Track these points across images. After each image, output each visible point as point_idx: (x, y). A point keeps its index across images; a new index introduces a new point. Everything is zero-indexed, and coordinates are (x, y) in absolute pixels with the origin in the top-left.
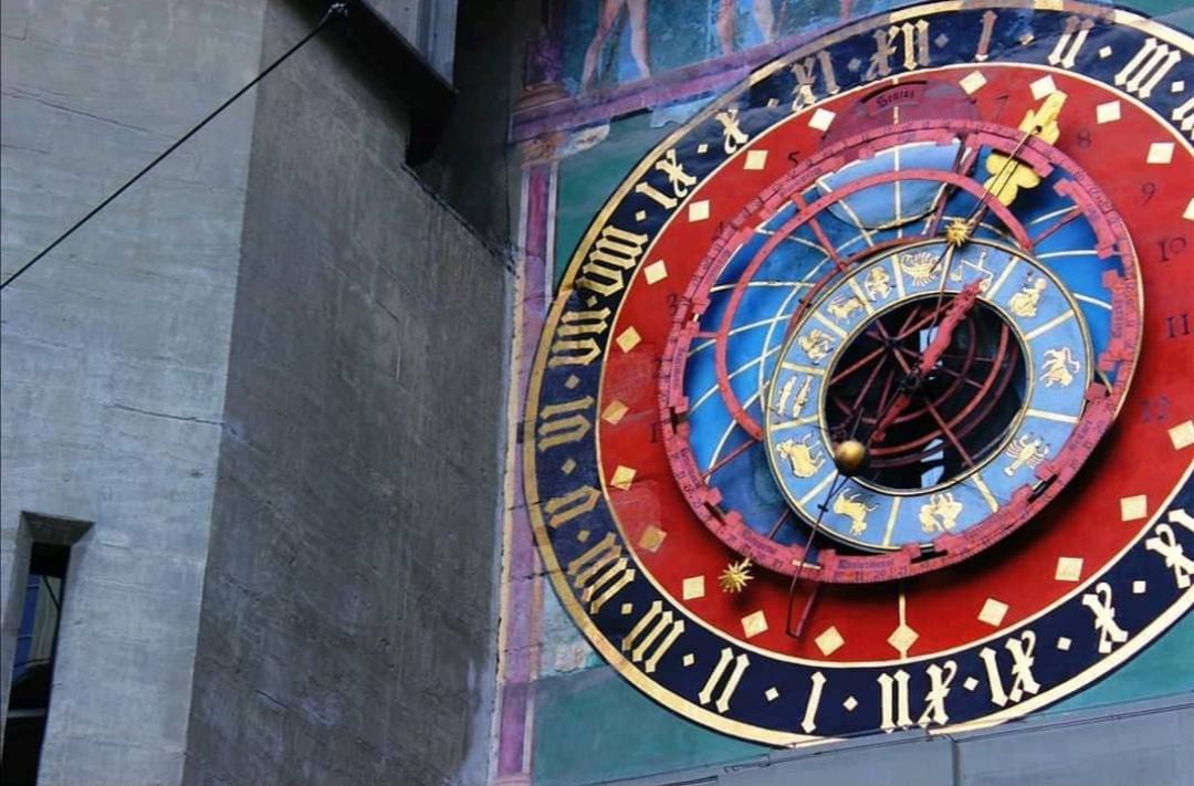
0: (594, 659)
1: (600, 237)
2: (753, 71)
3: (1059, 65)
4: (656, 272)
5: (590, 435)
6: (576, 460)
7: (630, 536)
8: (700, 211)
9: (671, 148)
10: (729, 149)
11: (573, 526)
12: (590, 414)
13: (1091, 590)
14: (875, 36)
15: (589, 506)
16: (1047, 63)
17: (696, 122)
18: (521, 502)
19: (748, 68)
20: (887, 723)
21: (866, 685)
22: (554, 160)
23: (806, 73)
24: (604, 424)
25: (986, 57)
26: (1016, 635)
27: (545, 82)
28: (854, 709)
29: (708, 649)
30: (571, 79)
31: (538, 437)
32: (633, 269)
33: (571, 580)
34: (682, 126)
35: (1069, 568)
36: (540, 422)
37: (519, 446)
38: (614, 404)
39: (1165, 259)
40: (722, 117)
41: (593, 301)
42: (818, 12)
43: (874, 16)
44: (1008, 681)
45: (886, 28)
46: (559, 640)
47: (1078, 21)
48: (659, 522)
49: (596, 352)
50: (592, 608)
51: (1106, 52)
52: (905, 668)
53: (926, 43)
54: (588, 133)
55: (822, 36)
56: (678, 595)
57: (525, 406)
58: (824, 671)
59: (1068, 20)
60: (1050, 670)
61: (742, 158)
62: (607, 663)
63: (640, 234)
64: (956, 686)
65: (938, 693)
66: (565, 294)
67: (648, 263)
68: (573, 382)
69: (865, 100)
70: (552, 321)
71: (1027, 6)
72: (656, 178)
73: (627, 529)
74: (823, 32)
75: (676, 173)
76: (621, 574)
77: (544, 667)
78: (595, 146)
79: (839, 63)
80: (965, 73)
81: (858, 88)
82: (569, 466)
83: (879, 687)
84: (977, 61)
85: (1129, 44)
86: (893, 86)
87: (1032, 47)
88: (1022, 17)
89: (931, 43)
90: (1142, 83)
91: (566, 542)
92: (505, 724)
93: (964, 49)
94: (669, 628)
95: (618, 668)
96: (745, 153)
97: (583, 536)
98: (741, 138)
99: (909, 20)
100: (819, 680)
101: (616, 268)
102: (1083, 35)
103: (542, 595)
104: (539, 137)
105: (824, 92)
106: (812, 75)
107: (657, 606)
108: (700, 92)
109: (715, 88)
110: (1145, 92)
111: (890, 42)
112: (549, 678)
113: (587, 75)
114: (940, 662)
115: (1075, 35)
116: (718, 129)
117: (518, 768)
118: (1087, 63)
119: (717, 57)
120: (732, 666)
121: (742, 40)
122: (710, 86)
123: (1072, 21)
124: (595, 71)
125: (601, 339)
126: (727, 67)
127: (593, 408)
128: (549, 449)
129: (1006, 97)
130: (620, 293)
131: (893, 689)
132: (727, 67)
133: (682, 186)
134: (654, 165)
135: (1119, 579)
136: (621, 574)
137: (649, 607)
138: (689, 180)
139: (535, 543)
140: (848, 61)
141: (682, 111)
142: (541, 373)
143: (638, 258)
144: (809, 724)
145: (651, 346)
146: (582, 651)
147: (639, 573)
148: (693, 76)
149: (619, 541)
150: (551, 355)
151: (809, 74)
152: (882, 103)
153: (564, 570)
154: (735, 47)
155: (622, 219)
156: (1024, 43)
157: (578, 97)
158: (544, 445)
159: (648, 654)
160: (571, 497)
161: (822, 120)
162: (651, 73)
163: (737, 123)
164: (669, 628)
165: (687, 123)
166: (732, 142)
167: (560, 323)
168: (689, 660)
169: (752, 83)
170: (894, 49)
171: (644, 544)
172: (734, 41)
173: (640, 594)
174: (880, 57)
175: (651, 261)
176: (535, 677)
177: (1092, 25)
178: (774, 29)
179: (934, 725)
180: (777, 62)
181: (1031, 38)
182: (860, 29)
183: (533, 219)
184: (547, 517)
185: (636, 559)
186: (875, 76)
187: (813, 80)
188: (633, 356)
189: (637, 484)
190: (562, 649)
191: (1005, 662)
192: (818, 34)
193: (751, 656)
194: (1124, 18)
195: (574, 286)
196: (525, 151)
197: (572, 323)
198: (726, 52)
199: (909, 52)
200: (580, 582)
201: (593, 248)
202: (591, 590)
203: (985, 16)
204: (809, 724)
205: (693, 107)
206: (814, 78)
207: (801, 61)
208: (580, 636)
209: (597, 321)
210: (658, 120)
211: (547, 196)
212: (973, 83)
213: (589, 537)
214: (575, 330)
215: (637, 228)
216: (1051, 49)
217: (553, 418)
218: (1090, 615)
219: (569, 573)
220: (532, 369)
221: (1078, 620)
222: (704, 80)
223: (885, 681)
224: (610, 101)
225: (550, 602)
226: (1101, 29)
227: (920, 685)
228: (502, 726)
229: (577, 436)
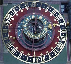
4: (13, 19)
8: (17, 15)
10: (19, 9)
12: (7, 31)
13: (49, 54)
15: (8, 39)
17: (16, 6)
20: (33, 62)
21: (32, 58)
24: (9, 32)
26: (43, 56)
28: (30, 60)
29: (19, 53)
31: (3, 32)
33: (6, 45)
35: (47, 52)
38: (9, 30)
40: (18, 6)
41: (7, 20)
44: (43, 60)
45: (33, 2)
46: (5, 50)
49: (8, 25)
51: (51, 10)
52: (35, 58)
54: (6, 4)
56: (16, 48)
58: (28, 57)
60: (46, 60)
64: (39, 60)
65: (37, 60)
66: (5, 19)
67: (12, 18)
70: (3, 21)
72: (12, 10)
75: (15, 10)
79: (29, 4)
82: (6, 35)
83: (32, 59)
85: (53, 9)
89: (37, 5)
91: (5, 41)
93: (39, 6)
94: (15, 51)
98: (20, 9)
99: (35, 2)
100: (28, 57)
102: (49, 8)
107: (14, 49)
110: (54, 14)
114: (37, 58)
116: (18, 7)
117: (2, 60)
118: (49, 10)
123: (48, 6)
125: (8, 24)
130: (10, 20)
131: (34, 59)
135: (51, 53)
138: (16, 11)
139: (3, 41)
141: (15, 4)
144: (27, 61)
149: (10, 42)
150: (3, 24)
152: (33, 9)
153: (5, 44)
155: (10, 13)
158: (3, 32)
160: (6, 38)
173: (12, 47)
174: (32, 4)
175: (13, 18)
176: (3, 53)
179: (37, 62)
184: (4, 39)
191: (42, 58)
199: (35, 5)
200: (7, 45)
202: (8, 46)
204: (27, 61)
205: (16, 4)
207: (25, 3)
210: (13, 5)
212: (40, 9)
214: (5, 22)
215: (11, 15)
217: (4, 30)
218: (49, 56)
221: (48, 56)
223: (33, 58)
225: (4, 46)
226: (50, 8)
227: (36, 59)
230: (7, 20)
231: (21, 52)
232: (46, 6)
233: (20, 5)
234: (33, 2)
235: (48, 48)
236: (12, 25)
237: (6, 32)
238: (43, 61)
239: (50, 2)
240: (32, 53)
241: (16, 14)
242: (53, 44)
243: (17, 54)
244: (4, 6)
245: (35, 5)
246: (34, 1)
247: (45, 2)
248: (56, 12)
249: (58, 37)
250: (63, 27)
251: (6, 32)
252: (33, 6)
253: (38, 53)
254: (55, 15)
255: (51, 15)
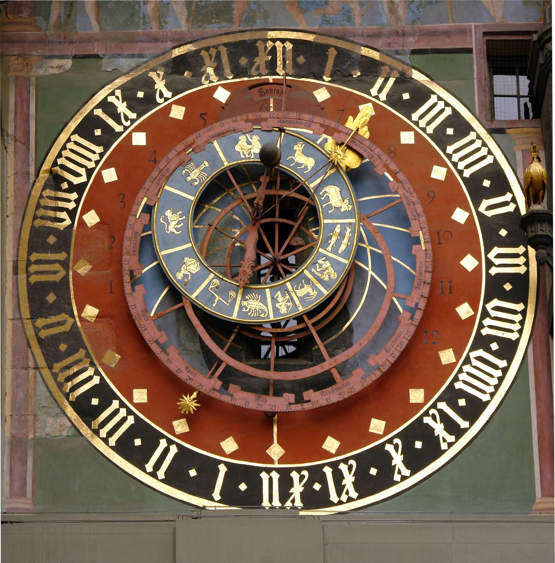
0: (72, 431)
1: (69, 140)
2: (174, 48)
3: (377, 97)
4: (110, 175)
5: (65, 279)
6: (56, 294)
7: (96, 354)
8: (140, 139)
9: (117, 88)
10: (159, 100)
11: (55, 339)
12: (65, 264)
14: (257, 44)
15: (66, 328)
16: (370, 94)
18: (17, 316)
19: (169, 44)
21: (253, 477)
22: (33, 76)
23: (211, 59)
24: (76, 274)
25: (330, 79)
27: (21, 15)
29: (152, 440)
30: (41, 18)
31: (28, 274)
32: (94, 169)
33: (55, 376)
34: (125, 74)
36: (29, 263)
37: (15, 276)
38: (81, 262)
39: (440, 243)
40: (153, 75)
41: (65, 186)
42: (218, 16)
43: (256, 30)
45: (265, 41)
46: (49, 414)
47: (389, 71)
48: (114, 348)
49: (68, 222)
50: (70, 397)
51: (406, 96)
53: (291, 58)
54: (56, 62)
55: (221, 35)
56: (131, 400)
57: (18, 249)
58: (227, 464)
59: (382, 68)
61: (168, 109)
62: (82, 435)
63: (98, 145)
66: (44, 176)
68: (52, 240)
69: (251, 88)
70: (36, 193)
71: (357, 51)
72: (105, 105)
73: (93, 348)
74: (222, 32)
75: (122, 107)
76: (90, 378)
77: (37, 430)
78: (60, 74)
79: (233, 58)
80: (319, 86)
81: (246, 79)
82: (51, 298)
84: (324, 81)
86: (268, 84)
87: (359, 80)
88: (353, 58)
89: (294, 60)
90: (428, 123)
91: (51, 349)
92: (12, 464)
93: (315, 70)
94: (124, 420)
95: (90, 439)
96: (170, 105)
97: (63, 347)
98: (168, 94)
99: (281, 38)
100: (223, 469)
101: (82, 166)
102: (391, 81)
103: (35, 381)
104: (20, 56)
105: (223, 75)
106: (214, 62)
107: (115, 404)
108: (137, 53)
109: (146, 52)
110: (430, 129)
111: (267, 51)
112: (41, 437)
113: (53, 18)
115: (386, 80)
116: (149, 85)
117: (23, 494)
118: (394, 99)
119: (149, 30)
120: (166, 451)
121: (166, 23)
122: (144, 50)
123: (385, 69)
124: (59, 17)
125: (72, 214)
126: (156, 39)
127: (68, 259)
128: (36, 283)
129: (343, 110)
130: (84, 185)
132: (156, 39)
133: (126, 118)
134: (106, 98)
136: (90, 378)
137: (110, 404)
140: (239, 58)
141: (125, 63)
142: (29, 228)
143: (97, 162)
145: (107, 226)
146: (64, 424)
147: (102, 379)
148: (132, 40)
149: (88, 355)
150: (35, 218)
151: (213, 59)
153: (50, 368)
154: (161, 27)
155: (86, 129)
156: (354, 76)
157: (48, 33)
158: (34, 279)
159: (111, 433)
160: (53, 319)
161: (222, 95)
162: (101, 29)
163: (163, 83)
164: (124, 420)
165: (128, 73)
166: (161, 95)
167: (41, 196)
168: (138, 442)
169: (174, 56)
170: (270, 57)
171: (105, 360)
172: (160, 21)
173: (104, 393)
174: (262, 59)
175: (106, 166)
176: (31, 436)
177: (398, 75)
178: (188, 21)
180: (191, 45)
181: (359, 74)
182: (247, 37)
183: (19, 116)
184: (37, 330)
185: (100, 370)
186: (257, 73)
187: (215, 64)
188: (94, 231)
189: (99, 319)
190: (50, 420)
192: (219, 33)
193: (179, 446)
194: (417, 76)
195: (51, 172)
196: (10, 63)
197: (50, 198)
198: (154, 28)
199: (279, 63)
201: (64, 148)
202: (69, 385)
203: (329, 50)
205: (132, 62)
206: (216, 63)
207: (207, 49)
208: (62, 415)
209: (69, 201)
210: (107, 65)
211: (28, 102)
212: (322, 95)
213: (67, 349)
214: (52, 203)
216: (372, 85)
219: (53, 371)
220: (22, 224)
222: (140, 45)
224: (71, 42)
225: (41, 388)
226: (404, 81)
228: (11, 465)
229: (57, 278)
230: (65, 180)
231: (172, 432)
232: (371, 69)
233: (165, 65)
234: (265, 41)
235: (384, 393)
236: (98, 220)
237: (55, 273)
238: (344, 498)
239: (404, 34)
240: (255, 429)
241: (130, 136)
242: (413, 363)
243: (138, 442)
244: (38, 79)
245: (284, 68)
246: (272, 34)
247: (362, 36)
248: (448, 112)
249: (459, 304)
250: (503, 233)
251: (55, 273)
252: (264, 70)
253: (303, 434)
254: (440, 136)
255: (407, 138)
